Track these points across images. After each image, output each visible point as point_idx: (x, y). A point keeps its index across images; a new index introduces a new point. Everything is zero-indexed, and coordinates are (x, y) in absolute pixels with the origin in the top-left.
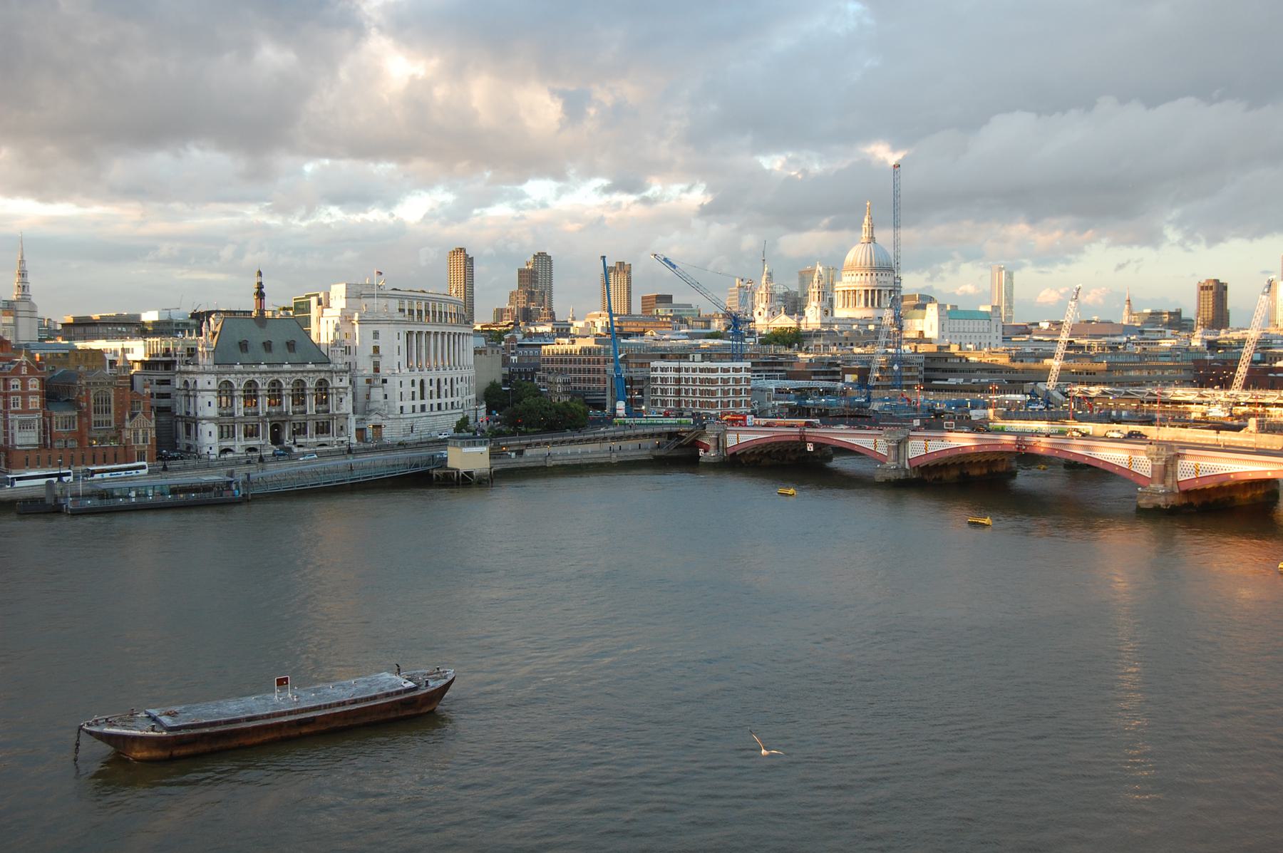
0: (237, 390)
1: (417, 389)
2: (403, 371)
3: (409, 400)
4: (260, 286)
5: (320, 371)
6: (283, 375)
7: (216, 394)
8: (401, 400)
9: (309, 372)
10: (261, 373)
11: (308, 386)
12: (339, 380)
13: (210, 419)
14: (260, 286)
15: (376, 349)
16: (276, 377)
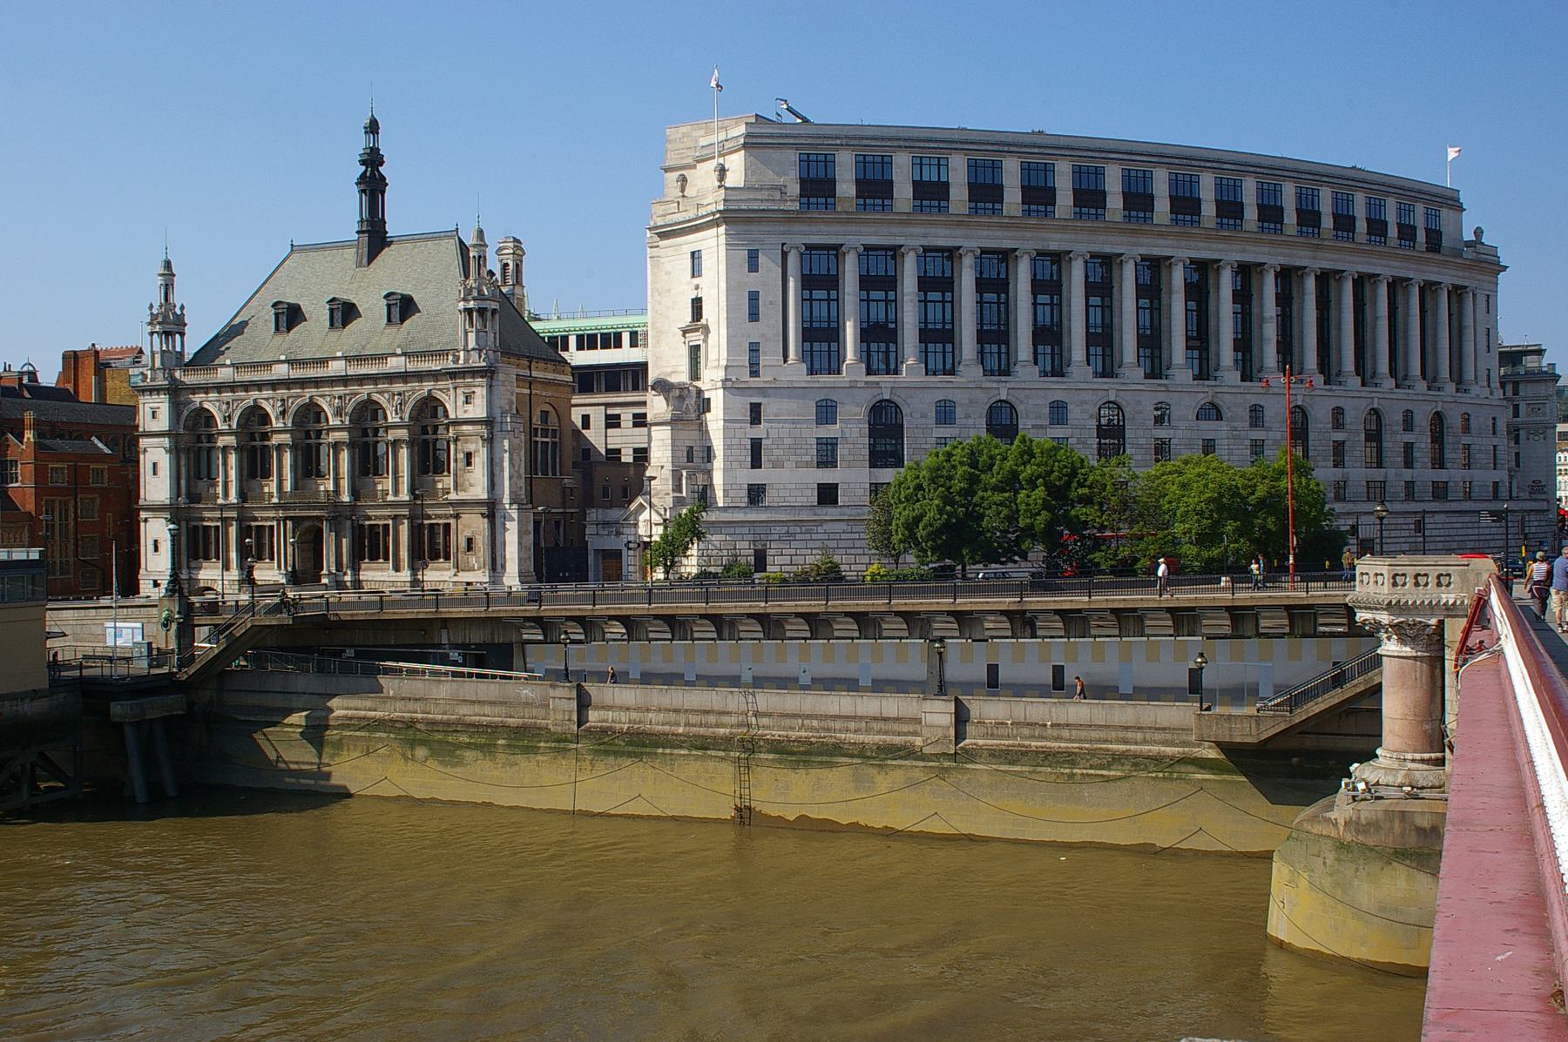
0: (222, 433)
1: (852, 430)
2: (765, 377)
3: (807, 465)
4: (373, 159)
5: (420, 376)
6: (326, 390)
7: (166, 441)
8: (756, 463)
9: (391, 378)
10: (220, 388)
11: (390, 420)
12: (461, 399)
13: (156, 509)
14: (373, 159)
15: (697, 304)
16: (365, 391)
